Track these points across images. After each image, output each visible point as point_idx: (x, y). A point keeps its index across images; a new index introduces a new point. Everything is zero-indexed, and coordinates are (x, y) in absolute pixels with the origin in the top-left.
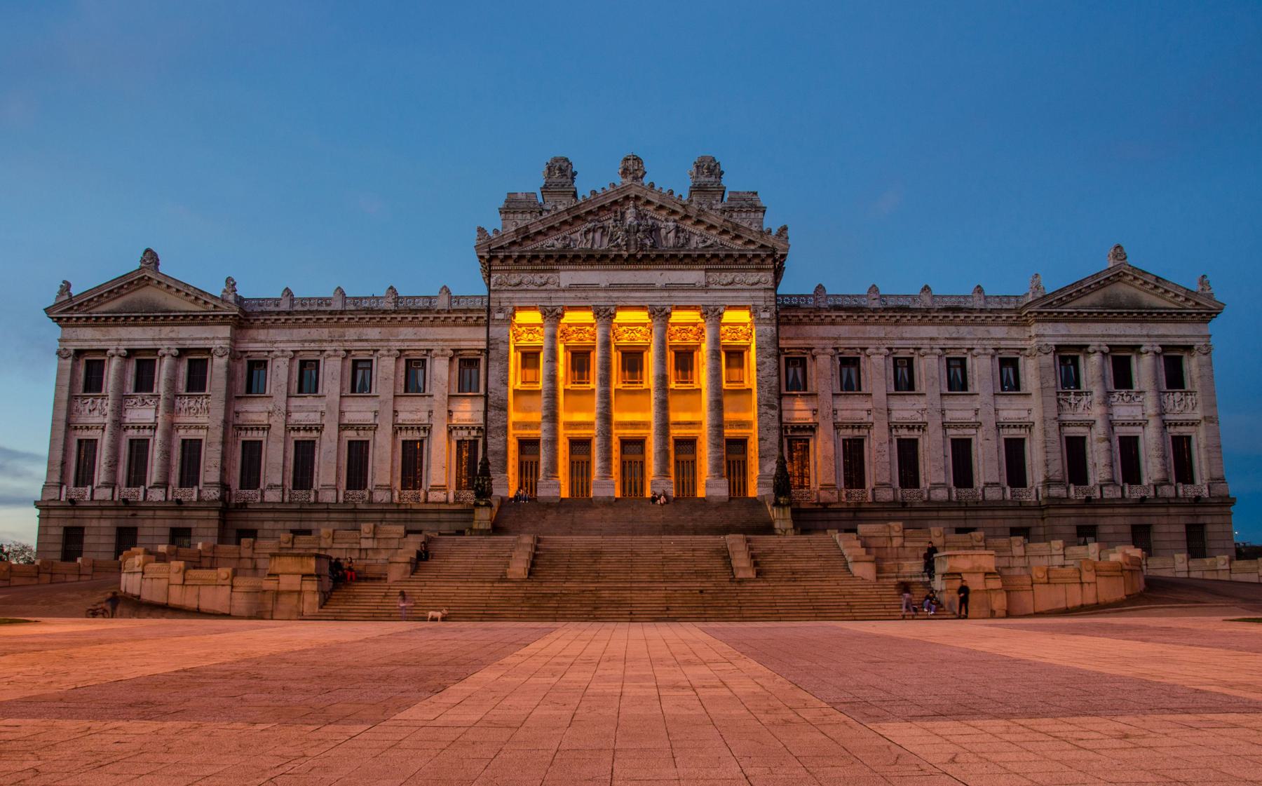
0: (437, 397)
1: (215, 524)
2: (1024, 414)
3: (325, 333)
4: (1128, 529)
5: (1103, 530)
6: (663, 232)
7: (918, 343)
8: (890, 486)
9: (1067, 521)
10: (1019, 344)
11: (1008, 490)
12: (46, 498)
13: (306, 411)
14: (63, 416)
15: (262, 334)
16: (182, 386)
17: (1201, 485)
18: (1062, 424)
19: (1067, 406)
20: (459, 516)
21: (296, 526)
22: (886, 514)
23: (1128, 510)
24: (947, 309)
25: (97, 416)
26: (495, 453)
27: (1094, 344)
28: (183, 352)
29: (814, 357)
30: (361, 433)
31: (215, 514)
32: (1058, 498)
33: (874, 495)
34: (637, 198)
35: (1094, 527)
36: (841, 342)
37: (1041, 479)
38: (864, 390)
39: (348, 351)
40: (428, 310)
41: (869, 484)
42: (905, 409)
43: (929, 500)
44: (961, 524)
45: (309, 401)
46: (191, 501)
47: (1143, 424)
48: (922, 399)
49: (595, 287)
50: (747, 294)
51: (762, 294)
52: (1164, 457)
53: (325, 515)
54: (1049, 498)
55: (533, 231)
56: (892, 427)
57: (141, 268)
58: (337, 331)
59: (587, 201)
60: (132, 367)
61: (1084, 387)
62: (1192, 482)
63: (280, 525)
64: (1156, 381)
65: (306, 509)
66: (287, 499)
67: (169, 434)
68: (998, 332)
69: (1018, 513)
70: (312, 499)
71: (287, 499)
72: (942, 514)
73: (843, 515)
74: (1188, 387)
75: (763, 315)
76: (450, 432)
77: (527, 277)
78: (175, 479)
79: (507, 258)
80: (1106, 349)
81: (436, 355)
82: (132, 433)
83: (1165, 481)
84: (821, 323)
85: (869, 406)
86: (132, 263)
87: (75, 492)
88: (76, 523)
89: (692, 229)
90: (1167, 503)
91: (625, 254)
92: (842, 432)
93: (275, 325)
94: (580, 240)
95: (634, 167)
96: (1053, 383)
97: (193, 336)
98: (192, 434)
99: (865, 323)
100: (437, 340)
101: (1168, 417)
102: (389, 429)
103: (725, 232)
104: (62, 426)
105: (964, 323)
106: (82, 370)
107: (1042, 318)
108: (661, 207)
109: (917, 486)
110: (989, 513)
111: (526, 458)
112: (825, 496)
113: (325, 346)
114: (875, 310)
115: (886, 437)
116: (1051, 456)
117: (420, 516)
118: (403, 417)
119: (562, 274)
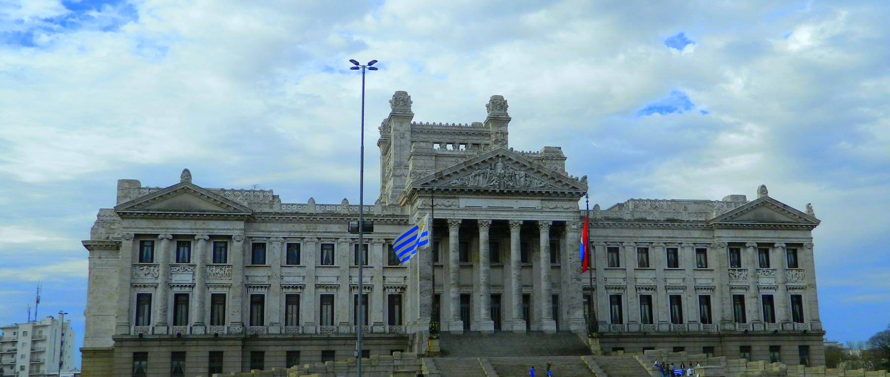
0: (376, 268)
1: (240, 348)
2: (710, 281)
3: (304, 227)
4: (768, 348)
5: (754, 349)
7: (651, 240)
8: (635, 322)
9: (734, 343)
10: (708, 241)
11: (702, 325)
12: (119, 333)
13: (293, 275)
14: (128, 278)
15: (262, 226)
16: (210, 260)
17: (806, 325)
18: (732, 288)
19: (733, 277)
20: (391, 341)
21: (290, 349)
22: (635, 339)
23: (767, 338)
24: (668, 220)
25: (153, 278)
27: (749, 242)
28: (212, 237)
29: (594, 247)
30: (329, 290)
31: (240, 343)
32: (731, 331)
34: (503, 156)
35: (750, 347)
37: (719, 319)
38: (622, 266)
39: (319, 239)
40: (372, 215)
41: (625, 321)
42: (645, 278)
43: (658, 331)
44: (676, 345)
45: (294, 270)
46: (223, 334)
47: (775, 288)
48: (653, 272)
49: (480, 208)
50: (564, 214)
51: (572, 214)
52: (787, 307)
53: (309, 342)
54: (724, 330)
56: (637, 288)
57: (182, 183)
58: (311, 226)
60: (174, 247)
61: (743, 267)
62: (802, 321)
63: (280, 348)
64: (782, 264)
65: (295, 339)
66: (283, 331)
67: (203, 291)
68: (696, 234)
69: (708, 339)
70: (300, 331)
71: (283, 331)
73: (612, 340)
74: (800, 267)
76: (384, 289)
78: (207, 320)
80: (756, 245)
82: (177, 290)
83: (787, 321)
84: (598, 227)
85: (624, 276)
86: (176, 180)
87: (141, 329)
88: (142, 350)
90: (789, 334)
91: (498, 191)
92: (609, 291)
93: (270, 221)
96: (726, 264)
97: (220, 228)
98: (219, 291)
99: (623, 228)
101: (789, 284)
102: (348, 289)
103: (553, 178)
104: (129, 286)
105: (677, 229)
106: (138, 247)
107: (721, 227)
110: (691, 339)
113: (304, 235)
114: (629, 220)
115: (635, 293)
116: (725, 306)
117: (369, 342)
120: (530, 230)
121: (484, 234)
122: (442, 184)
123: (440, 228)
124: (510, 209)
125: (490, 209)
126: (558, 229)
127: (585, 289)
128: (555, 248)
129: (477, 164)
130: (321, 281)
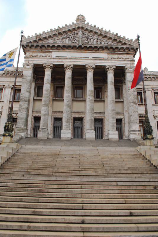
6: (92, 40)
26: (22, 118)
29: (145, 92)
34: (82, 28)
36: (154, 87)
49: (66, 58)
51: (129, 62)
55: (43, 37)
59: (63, 27)
75: (130, 69)
77: (39, 54)
79: (32, 46)
81: (6, 87)
91: (77, 46)
94: (59, 42)
95: (81, 18)
100: (7, 82)
103: (115, 40)
108: (91, 31)
111: (37, 124)
119: (53, 53)
120: (100, 73)
121: (68, 74)
122: (40, 43)
123: (38, 71)
124: (86, 58)
125: (73, 58)
126: (120, 73)
127: (140, 117)
128: (119, 90)
129: (64, 32)
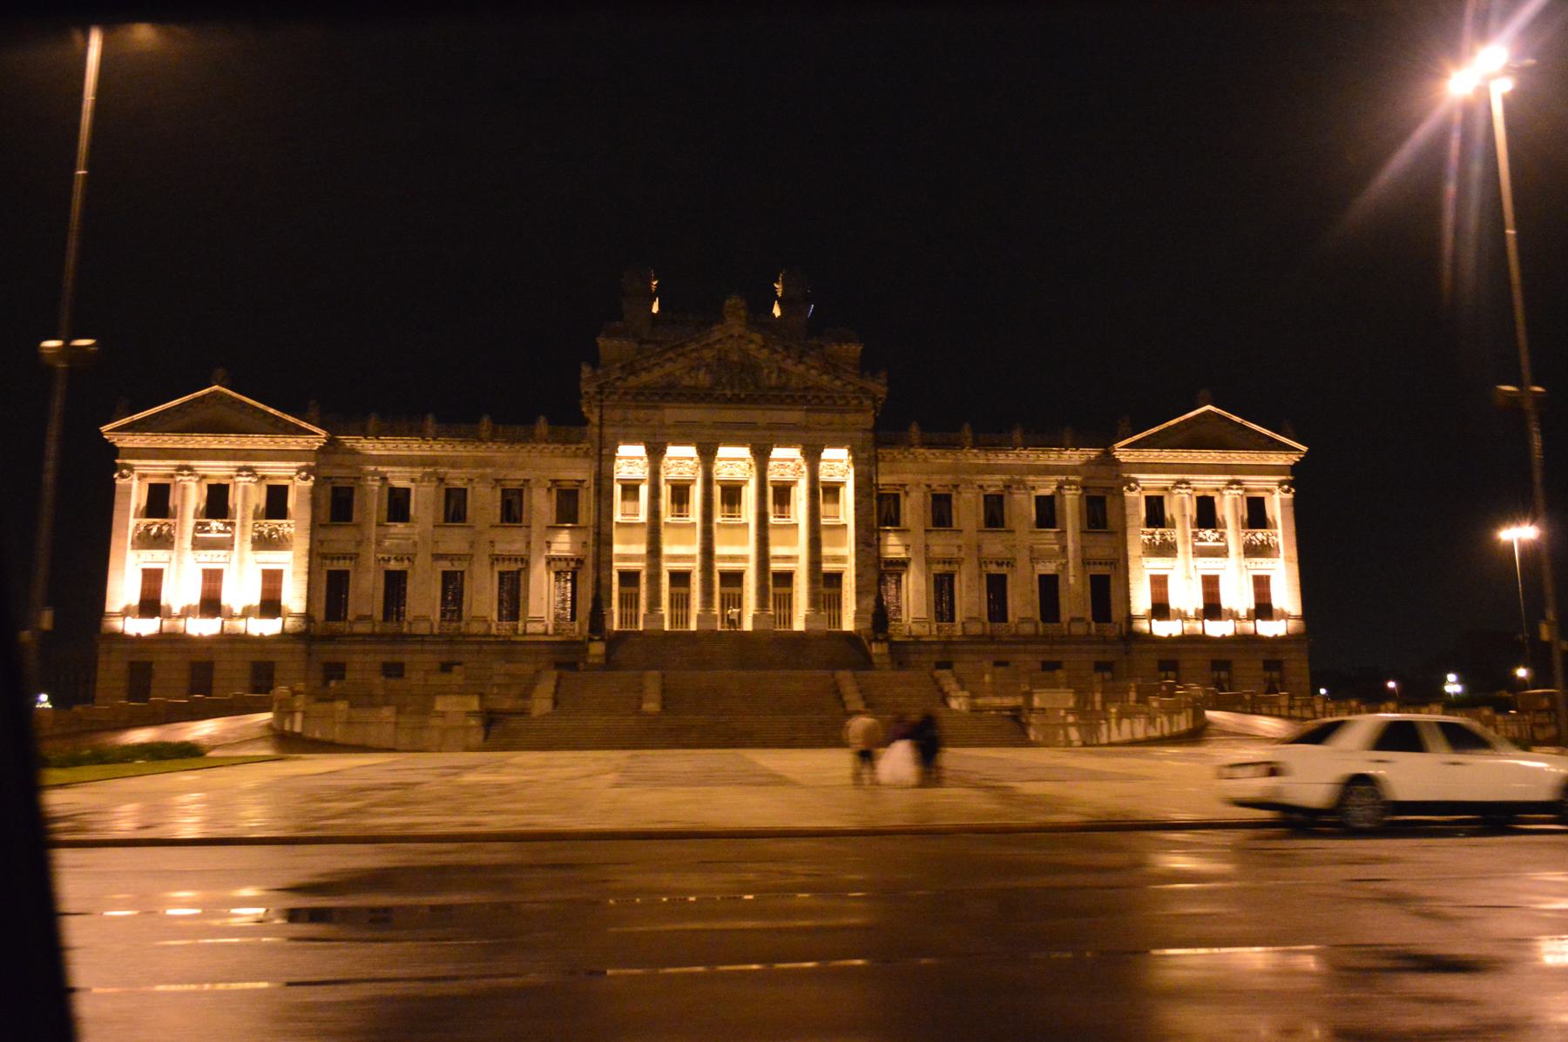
11: (1093, 625)
21: (386, 658)
29: (907, 493)
33: (964, 629)
44: (1047, 658)
45: (399, 528)
48: (1009, 536)
56: (982, 562)
72: (1029, 647)
76: (548, 563)
89: (792, 369)
102: (486, 561)
109: (1005, 620)
112: (916, 629)
115: (976, 572)
118: (500, 548)
130: (442, 549)
